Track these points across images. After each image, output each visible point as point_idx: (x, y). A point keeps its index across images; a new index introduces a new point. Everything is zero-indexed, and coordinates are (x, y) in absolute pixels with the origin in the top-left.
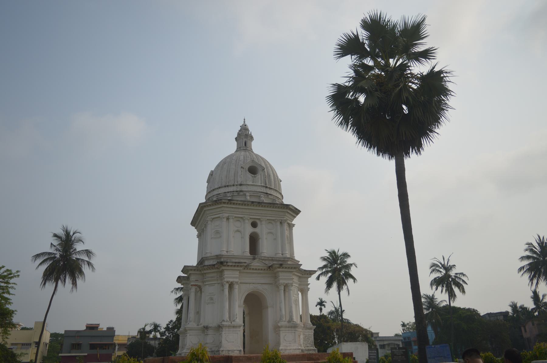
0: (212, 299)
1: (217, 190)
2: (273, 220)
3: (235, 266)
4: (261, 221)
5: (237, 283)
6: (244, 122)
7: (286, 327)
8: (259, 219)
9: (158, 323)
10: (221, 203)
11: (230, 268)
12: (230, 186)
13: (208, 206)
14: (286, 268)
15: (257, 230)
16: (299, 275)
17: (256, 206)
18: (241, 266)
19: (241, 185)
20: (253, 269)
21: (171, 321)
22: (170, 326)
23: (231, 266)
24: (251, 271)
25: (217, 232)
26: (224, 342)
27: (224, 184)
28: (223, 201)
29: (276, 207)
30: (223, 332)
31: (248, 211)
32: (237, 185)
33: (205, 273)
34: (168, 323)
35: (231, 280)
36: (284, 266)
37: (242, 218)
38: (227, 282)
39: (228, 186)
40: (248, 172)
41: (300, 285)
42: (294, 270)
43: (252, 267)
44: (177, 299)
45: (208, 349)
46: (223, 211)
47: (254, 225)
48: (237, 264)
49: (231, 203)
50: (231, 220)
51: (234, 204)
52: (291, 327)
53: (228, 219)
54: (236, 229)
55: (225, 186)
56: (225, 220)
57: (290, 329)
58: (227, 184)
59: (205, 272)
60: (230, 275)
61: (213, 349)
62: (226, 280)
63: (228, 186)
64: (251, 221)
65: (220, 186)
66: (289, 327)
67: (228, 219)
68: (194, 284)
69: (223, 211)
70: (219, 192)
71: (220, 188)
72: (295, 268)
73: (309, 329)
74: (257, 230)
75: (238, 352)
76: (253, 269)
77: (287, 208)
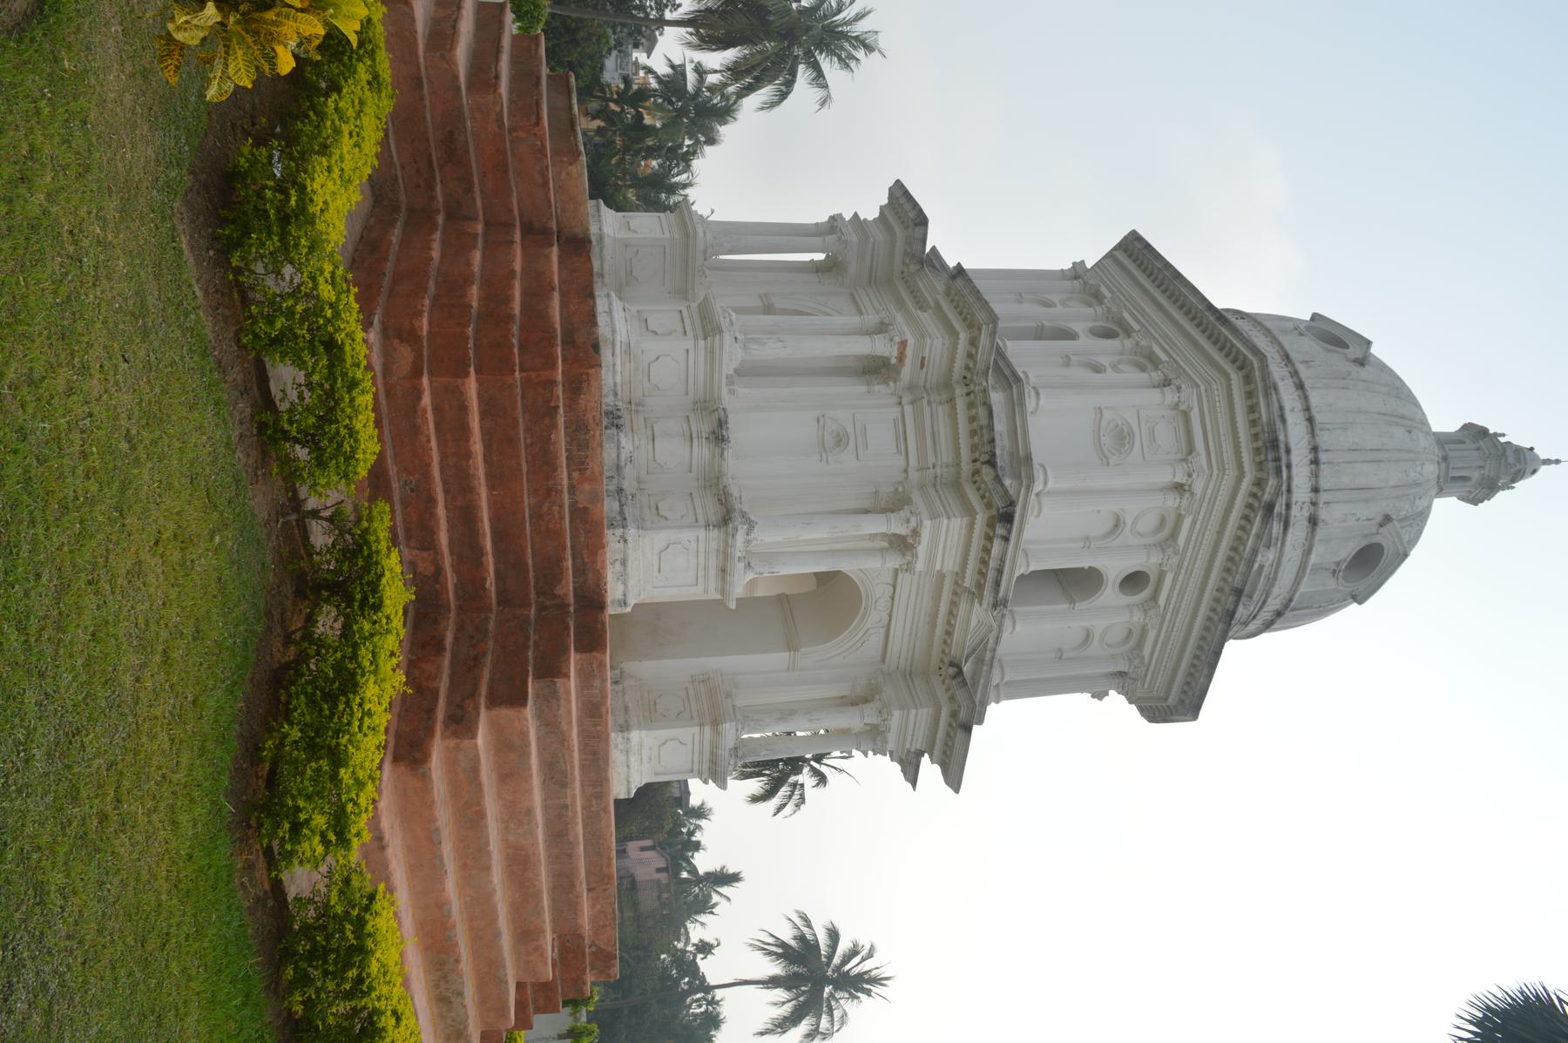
0: (841, 440)
1: (1299, 406)
3: (984, 562)
4: (1145, 607)
6: (1547, 462)
7: (714, 747)
8: (1154, 597)
10: (1260, 466)
12: (1315, 475)
13: (1250, 395)
15: (1110, 594)
19: (1313, 521)
20: (954, 604)
23: (987, 551)
25: (1123, 438)
26: (660, 538)
27: (1324, 439)
28: (1272, 482)
30: (702, 533)
31: (1200, 564)
32: (1314, 504)
33: (951, 400)
37: (1174, 536)
38: (916, 533)
39: (1315, 462)
40: (1364, 543)
43: (963, 606)
45: (626, 442)
46: (1222, 469)
47: (1134, 581)
48: (991, 575)
49: (1250, 506)
50: (1172, 501)
51: (1246, 518)
53: (1179, 488)
54: (1129, 521)
55: (1315, 449)
56: (1180, 478)
57: (707, 756)
58: (1323, 457)
59: (960, 404)
60: (945, 539)
61: (628, 471)
62: (927, 523)
63: (1315, 462)
65: (1318, 418)
68: (909, 351)
69: (1222, 469)
70: (1289, 417)
71: (1310, 420)
74: (1110, 594)
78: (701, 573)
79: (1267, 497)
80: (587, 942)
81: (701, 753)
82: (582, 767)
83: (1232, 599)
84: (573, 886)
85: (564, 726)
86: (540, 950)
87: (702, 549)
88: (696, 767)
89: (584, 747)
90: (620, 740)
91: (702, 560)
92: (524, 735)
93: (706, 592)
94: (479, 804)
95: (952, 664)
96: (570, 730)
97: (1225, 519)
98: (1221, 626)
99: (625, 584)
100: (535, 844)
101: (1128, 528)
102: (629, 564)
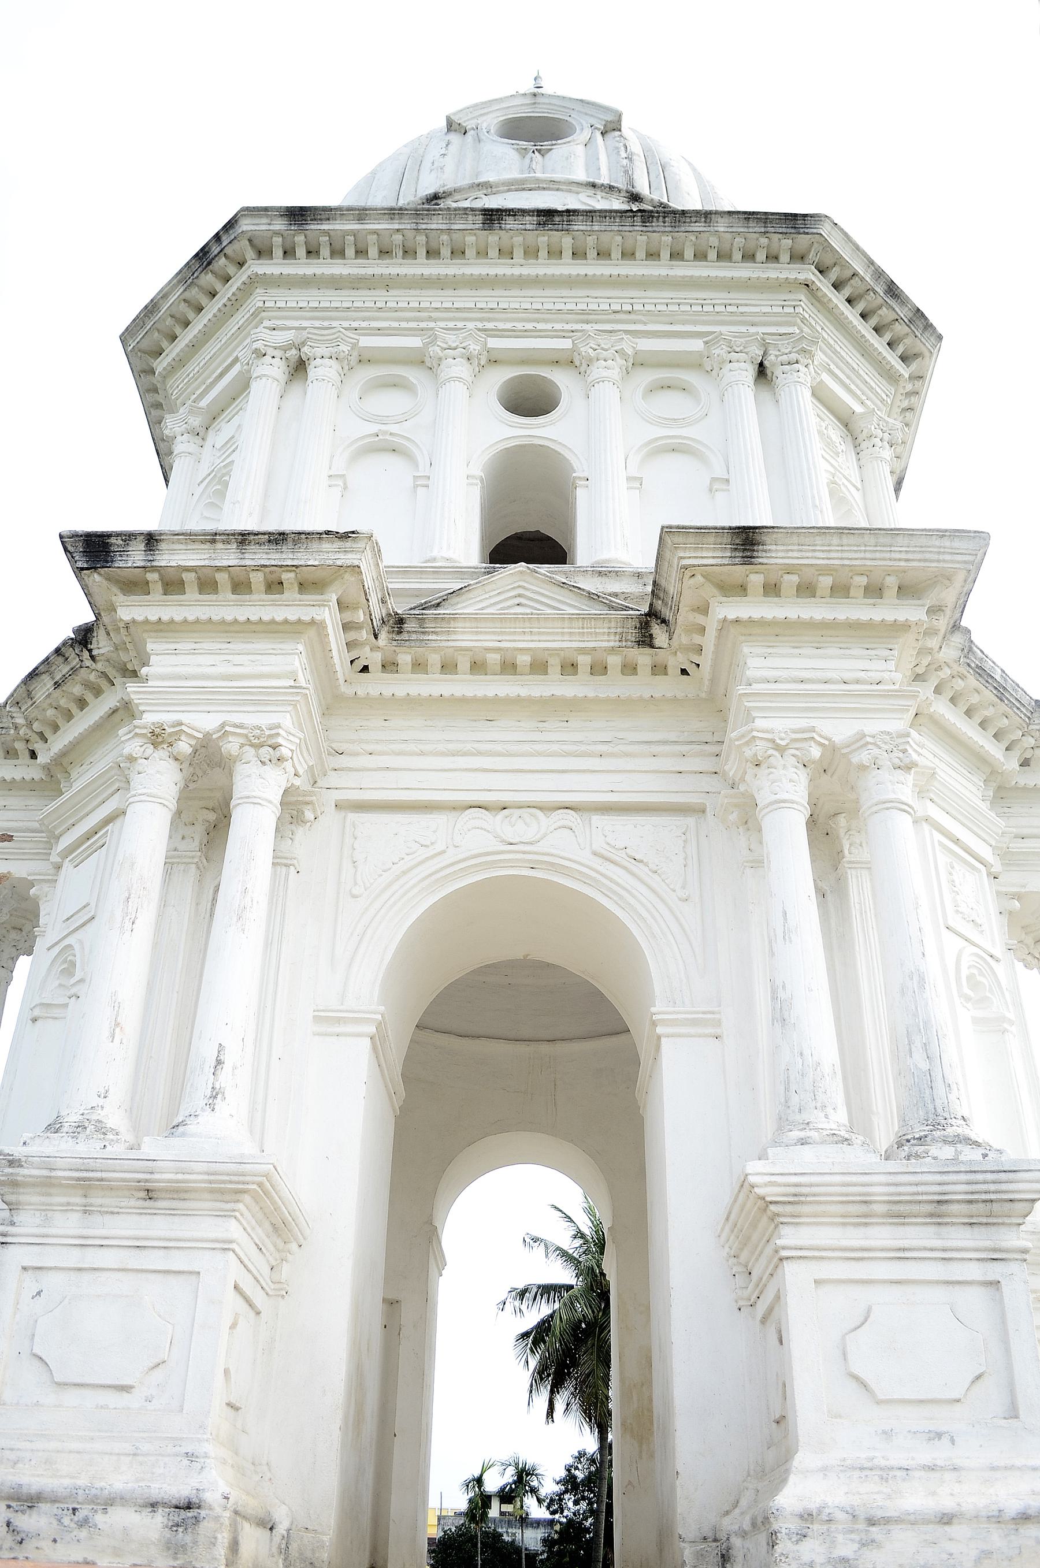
2: (695, 363)
5: (266, 745)
7: (860, 1210)
9: (529, 1458)
11: (189, 608)
14: (807, 590)
16: (994, 750)
17: (531, 253)
18: (311, 584)
21: (581, 1455)
22: (580, 1475)
24: (463, 686)
29: (700, 256)
31: (465, 300)
34: (570, 1461)
35: (204, 721)
36: (775, 555)
38: (157, 738)
41: (1007, 856)
42: (912, 613)
43: (465, 639)
44: (525, 1335)
47: (530, 401)
48: (259, 556)
51: (338, 252)
52: (937, 1210)
54: (374, 428)
57: (919, 1235)
64: (500, 377)
66: (898, 1214)
67: (299, 368)
72: (906, 591)
76: (477, 667)
77: (798, 257)
78: (154, 1260)
79: (280, 225)
81: (901, 1254)
83: (510, 222)
88: (974, 1271)
93: (225, 1246)
95: (646, 640)
99: (108, 1502)
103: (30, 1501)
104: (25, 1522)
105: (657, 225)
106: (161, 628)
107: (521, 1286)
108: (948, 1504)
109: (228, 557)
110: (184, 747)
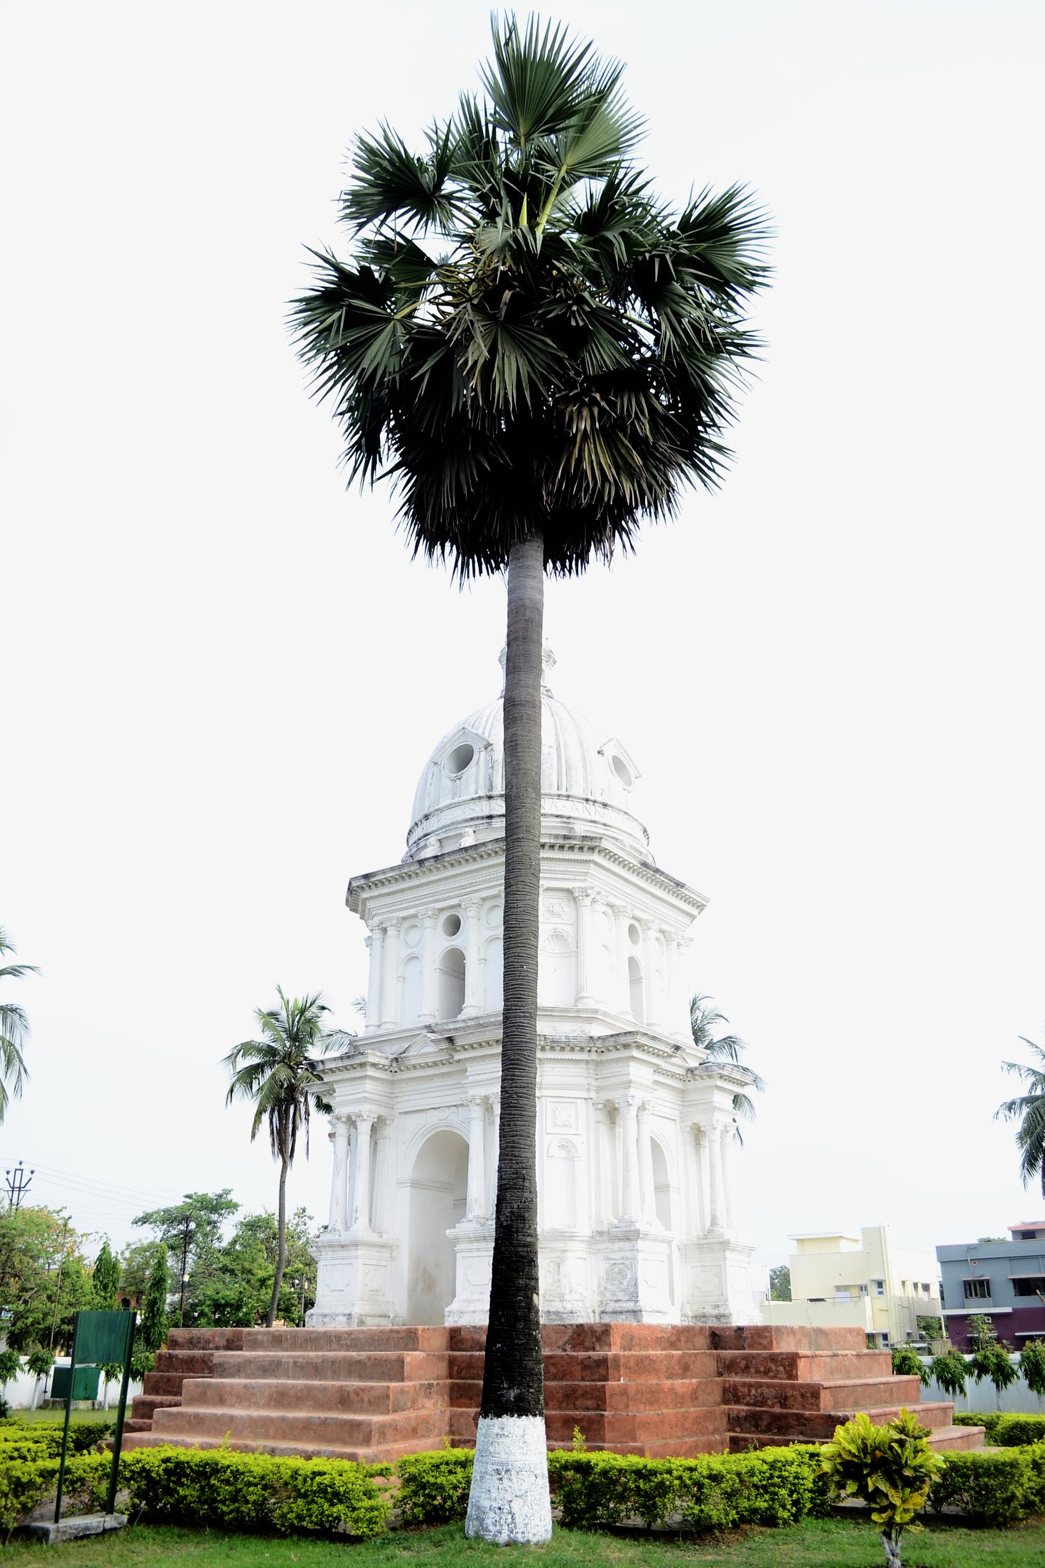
7: (470, 1240)
31: (425, 891)
36: (459, 1042)
43: (414, 1062)
48: (347, 1062)
50: (391, 931)
73: (620, 1240)
75: (344, 1319)
78: (345, 1261)
79: (363, 882)
80: (560, 1352)
81: (478, 1250)
82: (316, 1350)
83: (427, 864)
84: (359, 1362)
85: (241, 1360)
86: (358, 1392)
87: (331, 1262)
89: (303, 1348)
90: (450, 1319)
91: (337, 1262)
92: (197, 1385)
94: (190, 1416)
96: (243, 1356)
97: (393, 893)
98: (447, 859)
100: (269, 1386)
101: (414, 950)
102: (326, 1312)
103: (325, 1316)
104: (325, 1320)
105: (470, 852)
106: (335, 1081)
107: (1009, 1100)
108: (475, 1309)
109: (340, 1064)
110: (344, 1119)
